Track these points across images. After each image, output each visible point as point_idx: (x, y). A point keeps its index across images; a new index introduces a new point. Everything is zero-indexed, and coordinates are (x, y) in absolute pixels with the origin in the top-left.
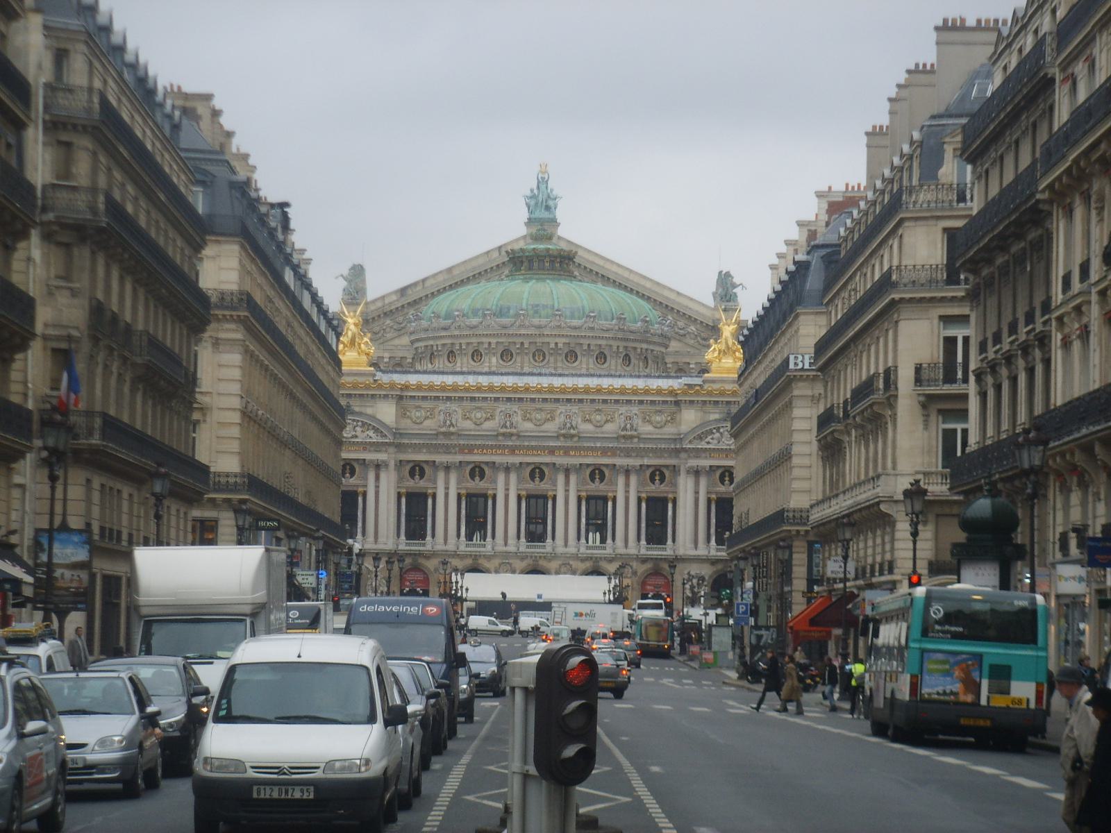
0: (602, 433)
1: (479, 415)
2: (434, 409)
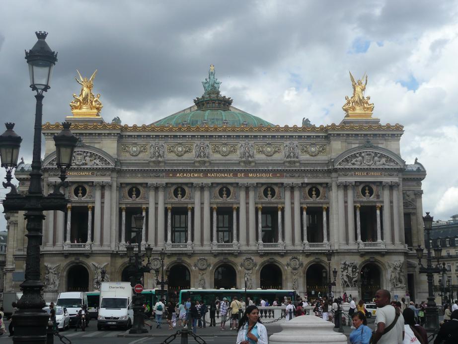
0: (272, 160)
1: (180, 149)
2: (147, 145)
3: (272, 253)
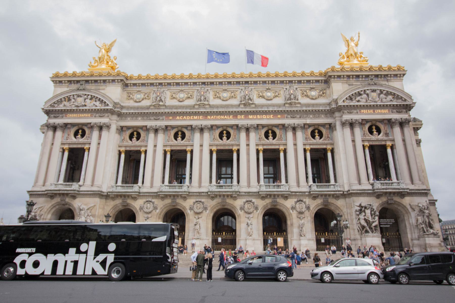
2: (150, 93)
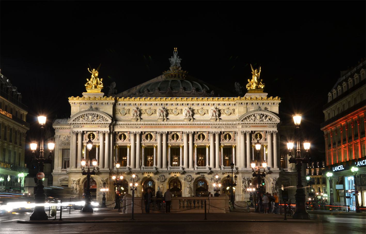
3: (202, 173)
